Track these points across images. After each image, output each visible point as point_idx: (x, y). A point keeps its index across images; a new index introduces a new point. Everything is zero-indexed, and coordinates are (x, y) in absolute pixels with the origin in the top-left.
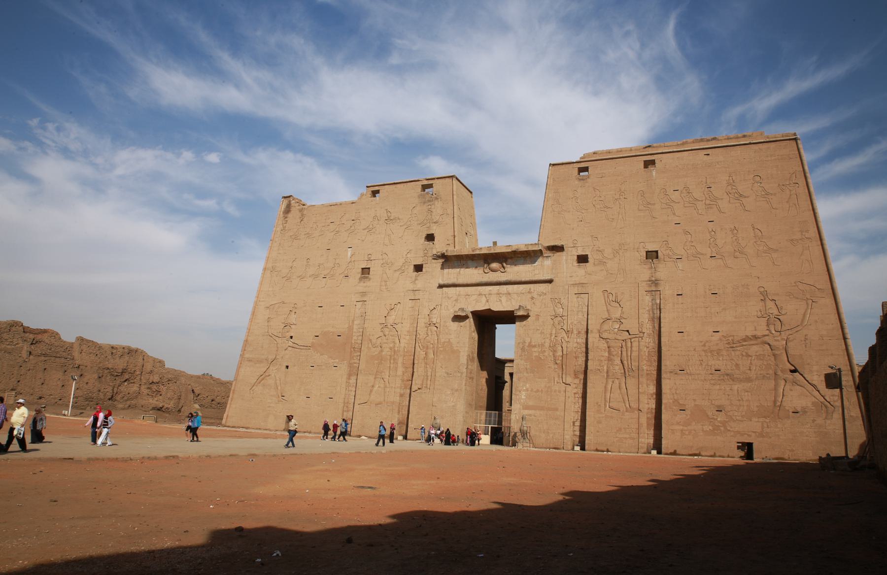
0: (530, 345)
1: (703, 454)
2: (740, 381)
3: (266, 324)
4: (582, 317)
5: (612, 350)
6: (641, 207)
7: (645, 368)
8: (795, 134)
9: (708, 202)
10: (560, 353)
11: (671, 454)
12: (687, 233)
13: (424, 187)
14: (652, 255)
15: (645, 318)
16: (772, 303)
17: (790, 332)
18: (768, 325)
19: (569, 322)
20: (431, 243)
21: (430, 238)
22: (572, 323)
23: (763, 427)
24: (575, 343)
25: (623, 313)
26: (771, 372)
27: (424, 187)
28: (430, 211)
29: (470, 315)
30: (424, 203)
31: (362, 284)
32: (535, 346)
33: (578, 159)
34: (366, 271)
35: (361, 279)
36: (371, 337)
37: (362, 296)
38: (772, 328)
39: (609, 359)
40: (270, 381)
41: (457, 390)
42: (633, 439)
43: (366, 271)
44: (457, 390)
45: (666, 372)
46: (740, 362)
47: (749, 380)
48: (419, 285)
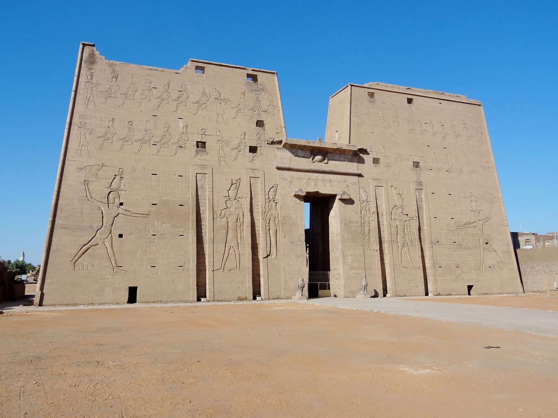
1: (453, 294)
9: (442, 134)
11: (438, 295)
13: (249, 76)
17: (485, 221)
21: (260, 124)
27: (249, 76)
30: (252, 91)
31: (199, 156)
32: (353, 222)
34: (201, 145)
35: (197, 152)
40: (99, 251)
41: (300, 256)
43: (201, 145)
44: (300, 256)
47: (469, 248)
48: (257, 164)
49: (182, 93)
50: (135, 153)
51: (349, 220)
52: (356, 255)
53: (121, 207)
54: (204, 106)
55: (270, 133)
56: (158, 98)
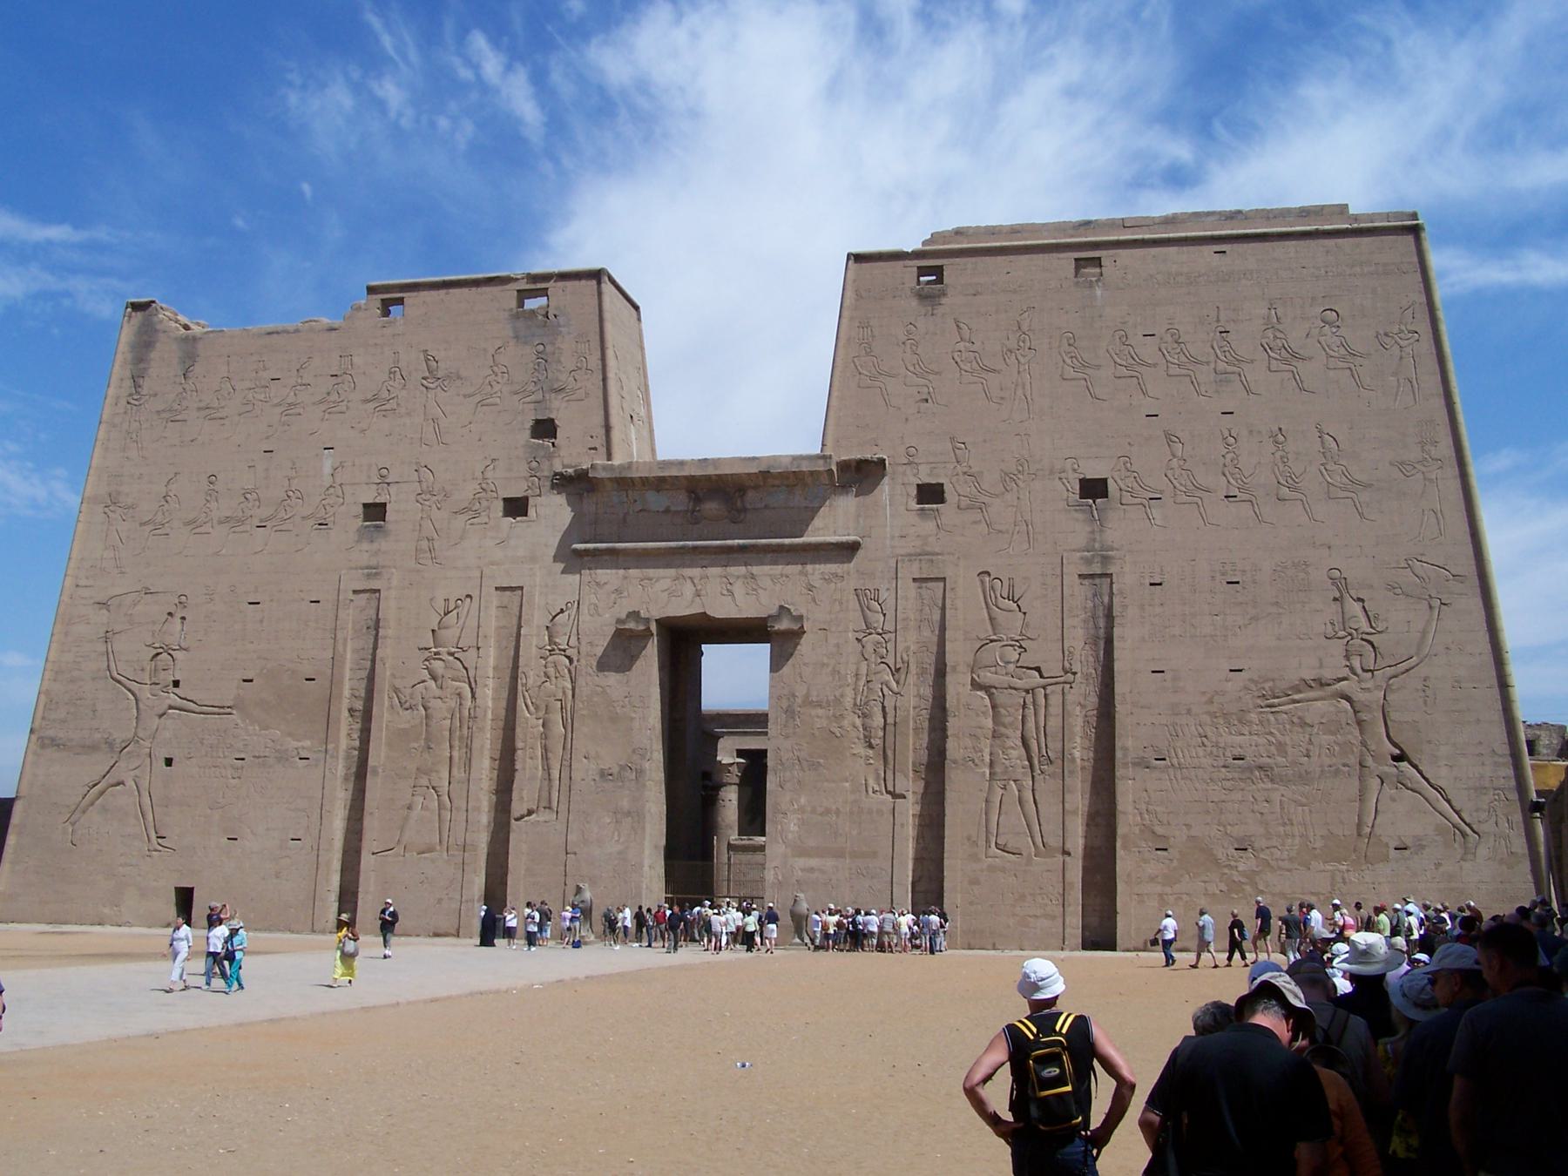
0: (808, 702)
2: (1284, 781)
3: (101, 648)
4: (930, 636)
5: (1003, 711)
6: (1070, 373)
7: (1077, 754)
8: (1414, 216)
9: (1221, 366)
10: (878, 720)
11: (1136, 950)
12: (1170, 438)
13: (523, 295)
14: (1094, 489)
15: (1077, 638)
16: (1357, 607)
18: (1347, 657)
19: (900, 647)
20: (547, 443)
21: (545, 429)
22: (908, 649)
23: (1333, 885)
24: (913, 697)
25: (1025, 625)
26: (1353, 760)
28: (543, 359)
29: (653, 628)
31: (365, 546)
33: (918, 246)
34: (375, 512)
35: (363, 535)
36: (398, 683)
37: (369, 576)
38: (1356, 663)
39: (995, 735)
40: (123, 799)
41: (629, 814)
42: (1053, 918)
43: (375, 512)
44: (629, 814)
45: (1126, 765)
46: (1287, 739)
47: (1304, 778)
49: (339, 380)
50: (217, 554)
51: (807, 696)
52: (820, 810)
53: (176, 690)
54: (393, 404)
55: (571, 453)
56: (279, 405)
